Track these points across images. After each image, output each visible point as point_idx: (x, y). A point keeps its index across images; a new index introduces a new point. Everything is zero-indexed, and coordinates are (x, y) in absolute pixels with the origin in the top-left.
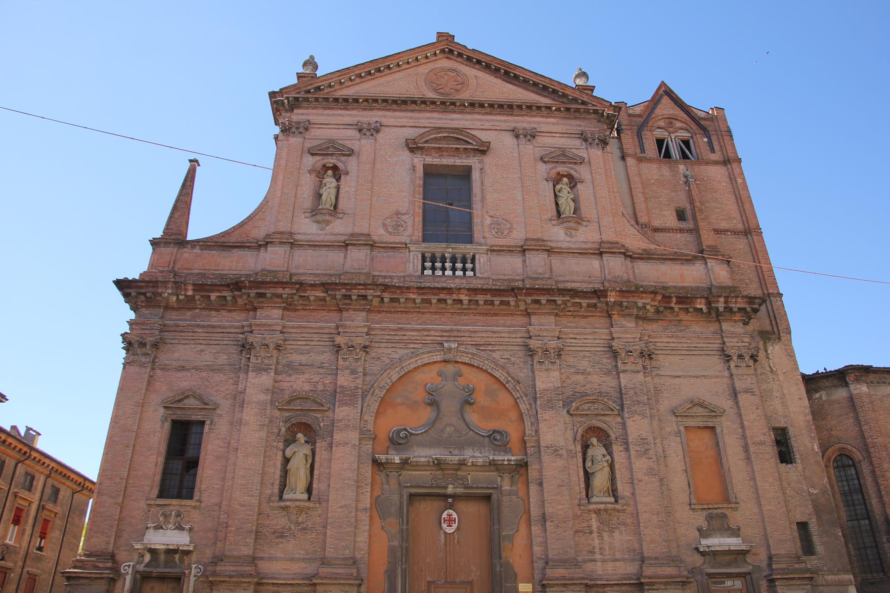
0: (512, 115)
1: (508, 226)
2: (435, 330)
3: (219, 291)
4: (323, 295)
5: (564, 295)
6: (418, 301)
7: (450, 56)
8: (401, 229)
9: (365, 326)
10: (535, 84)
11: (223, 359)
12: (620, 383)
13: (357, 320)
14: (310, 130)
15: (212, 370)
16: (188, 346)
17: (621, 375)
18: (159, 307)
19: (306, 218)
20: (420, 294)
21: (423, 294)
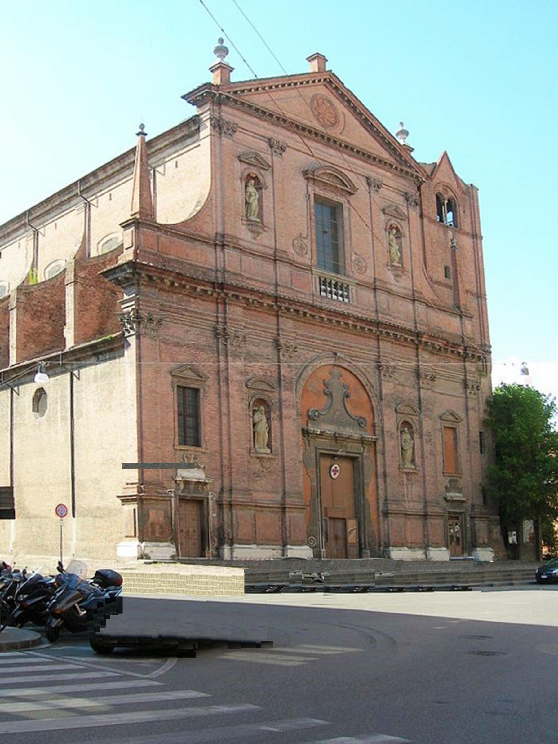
0: (366, 162)
1: (364, 264)
2: (331, 342)
3: (204, 285)
4: (272, 304)
5: (402, 332)
6: (325, 319)
7: (327, 85)
8: (305, 251)
9: (295, 332)
10: (383, 138)
11: (202, 341)
12: (419, 395)
13: (288, 324)
14: (237, 132)
15: (198, 349)
16: (178, 325)
17: (422, 390)
18: (156, 287)
19: (243, 224)
20: (327, 315)
21: (330, 315)
